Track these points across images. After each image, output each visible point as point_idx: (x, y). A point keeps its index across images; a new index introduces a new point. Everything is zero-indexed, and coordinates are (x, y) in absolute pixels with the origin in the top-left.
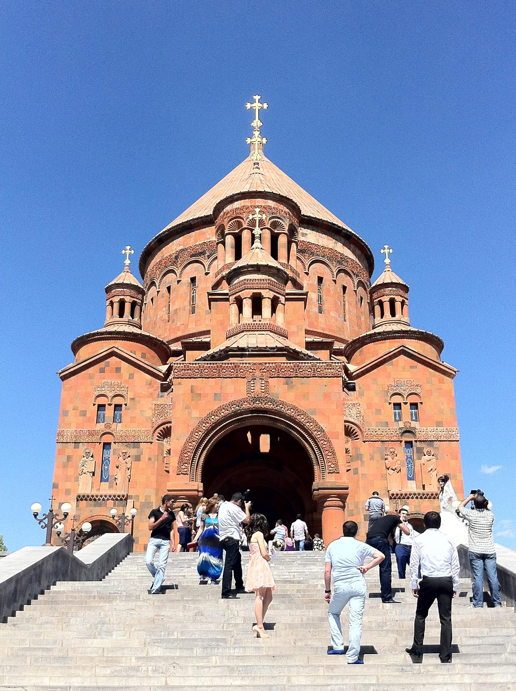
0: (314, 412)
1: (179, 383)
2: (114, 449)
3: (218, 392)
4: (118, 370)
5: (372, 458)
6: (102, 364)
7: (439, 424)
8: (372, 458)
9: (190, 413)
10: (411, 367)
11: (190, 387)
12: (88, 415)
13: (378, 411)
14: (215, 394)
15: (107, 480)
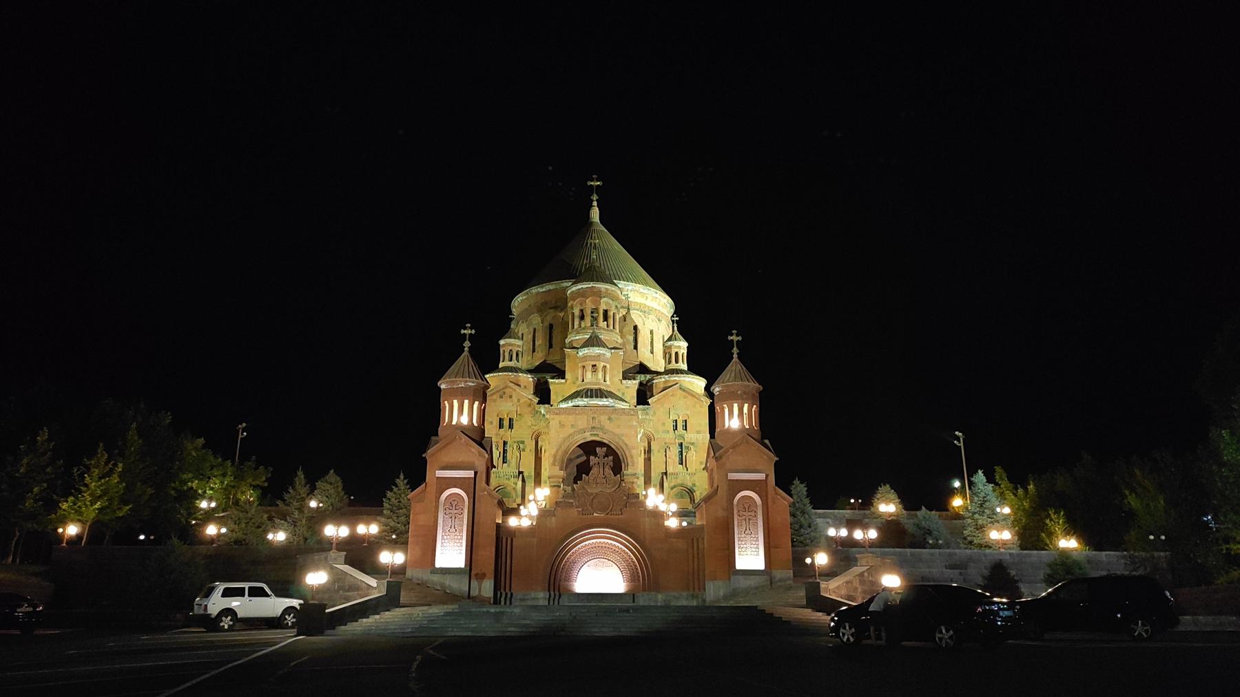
0: (623, 435)
1: (553, 419)
2: (510, 445)
3: (573, 424)
4: (511, 397)
5: (659, 452)
6: (501, 393)
7: (698, 432)
8: (659, 452)
9: (559, 435)
10: (684, 398)
11: (558, 422)
12: (494, 423)
13: (664, 424)
14: (572, 425)
15: (506, 463)
